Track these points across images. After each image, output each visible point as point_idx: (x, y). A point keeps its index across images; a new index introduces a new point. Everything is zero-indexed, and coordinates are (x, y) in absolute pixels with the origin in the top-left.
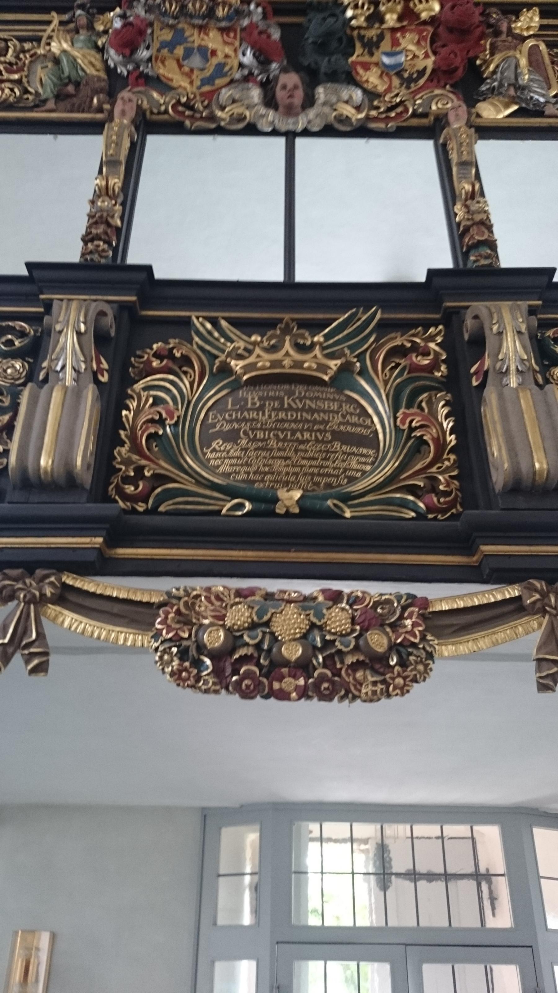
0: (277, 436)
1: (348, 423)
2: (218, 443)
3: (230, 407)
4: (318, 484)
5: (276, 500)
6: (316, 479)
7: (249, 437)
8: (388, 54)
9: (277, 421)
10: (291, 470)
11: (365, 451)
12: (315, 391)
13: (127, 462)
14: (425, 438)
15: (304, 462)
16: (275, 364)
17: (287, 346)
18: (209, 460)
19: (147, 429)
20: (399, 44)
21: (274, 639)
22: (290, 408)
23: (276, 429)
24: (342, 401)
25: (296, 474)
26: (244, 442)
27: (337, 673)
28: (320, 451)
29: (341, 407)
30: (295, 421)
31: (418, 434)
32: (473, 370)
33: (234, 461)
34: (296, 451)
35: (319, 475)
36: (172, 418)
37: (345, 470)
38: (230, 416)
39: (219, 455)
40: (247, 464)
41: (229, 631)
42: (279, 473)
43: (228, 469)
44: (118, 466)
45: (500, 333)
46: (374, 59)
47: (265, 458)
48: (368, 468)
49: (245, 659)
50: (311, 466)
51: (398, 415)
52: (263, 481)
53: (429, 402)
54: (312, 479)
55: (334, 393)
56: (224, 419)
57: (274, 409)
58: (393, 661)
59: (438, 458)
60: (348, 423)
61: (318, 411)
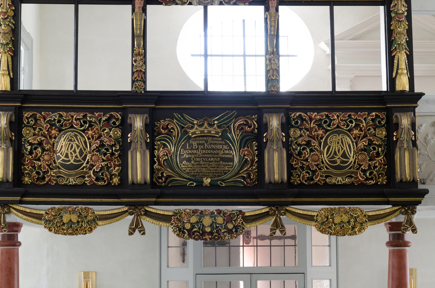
0: (203, 159)
2: (185, 162)
3: (188, 148)
4: (215, 176)
6: (215, 174)
7: (194, 160)
9: (203, 154)
10: (207, 171)
12: (215, 139)
13: (158, 170)
14: (248, 159)
15: (211, 169)
16: (202, 132)
17: (206, 124)
18: (182, 168)
19: (163, 157)
22: (207, 149)
23: (203, 157)
24: (223, 144)
25: (209, 173)
26: (193, 162)
28: (216, 165)
29: (223, 147)
30: (209, 154)
31: (246, 158)
32: (264, 135)
33: (190, 169)
34: (209, 165)
35: (216, 173)
36: (170, 155)
37: (224, 170)
38: (188, 152)
39: (185, 166)
40: (194, 170)
42: (204, 172)
43: (189, 171)
44: (155, 171)
45: (272, 129)
47: (199, 167)
48: (231, 169)
50: (213, 170)
51: (240, 151)
52: (199, 175)
53: (251, 145)
54: (214, 174)
55: (221, 140)
56: (186, 153)
57: (202, 149)
59: (252, 165)
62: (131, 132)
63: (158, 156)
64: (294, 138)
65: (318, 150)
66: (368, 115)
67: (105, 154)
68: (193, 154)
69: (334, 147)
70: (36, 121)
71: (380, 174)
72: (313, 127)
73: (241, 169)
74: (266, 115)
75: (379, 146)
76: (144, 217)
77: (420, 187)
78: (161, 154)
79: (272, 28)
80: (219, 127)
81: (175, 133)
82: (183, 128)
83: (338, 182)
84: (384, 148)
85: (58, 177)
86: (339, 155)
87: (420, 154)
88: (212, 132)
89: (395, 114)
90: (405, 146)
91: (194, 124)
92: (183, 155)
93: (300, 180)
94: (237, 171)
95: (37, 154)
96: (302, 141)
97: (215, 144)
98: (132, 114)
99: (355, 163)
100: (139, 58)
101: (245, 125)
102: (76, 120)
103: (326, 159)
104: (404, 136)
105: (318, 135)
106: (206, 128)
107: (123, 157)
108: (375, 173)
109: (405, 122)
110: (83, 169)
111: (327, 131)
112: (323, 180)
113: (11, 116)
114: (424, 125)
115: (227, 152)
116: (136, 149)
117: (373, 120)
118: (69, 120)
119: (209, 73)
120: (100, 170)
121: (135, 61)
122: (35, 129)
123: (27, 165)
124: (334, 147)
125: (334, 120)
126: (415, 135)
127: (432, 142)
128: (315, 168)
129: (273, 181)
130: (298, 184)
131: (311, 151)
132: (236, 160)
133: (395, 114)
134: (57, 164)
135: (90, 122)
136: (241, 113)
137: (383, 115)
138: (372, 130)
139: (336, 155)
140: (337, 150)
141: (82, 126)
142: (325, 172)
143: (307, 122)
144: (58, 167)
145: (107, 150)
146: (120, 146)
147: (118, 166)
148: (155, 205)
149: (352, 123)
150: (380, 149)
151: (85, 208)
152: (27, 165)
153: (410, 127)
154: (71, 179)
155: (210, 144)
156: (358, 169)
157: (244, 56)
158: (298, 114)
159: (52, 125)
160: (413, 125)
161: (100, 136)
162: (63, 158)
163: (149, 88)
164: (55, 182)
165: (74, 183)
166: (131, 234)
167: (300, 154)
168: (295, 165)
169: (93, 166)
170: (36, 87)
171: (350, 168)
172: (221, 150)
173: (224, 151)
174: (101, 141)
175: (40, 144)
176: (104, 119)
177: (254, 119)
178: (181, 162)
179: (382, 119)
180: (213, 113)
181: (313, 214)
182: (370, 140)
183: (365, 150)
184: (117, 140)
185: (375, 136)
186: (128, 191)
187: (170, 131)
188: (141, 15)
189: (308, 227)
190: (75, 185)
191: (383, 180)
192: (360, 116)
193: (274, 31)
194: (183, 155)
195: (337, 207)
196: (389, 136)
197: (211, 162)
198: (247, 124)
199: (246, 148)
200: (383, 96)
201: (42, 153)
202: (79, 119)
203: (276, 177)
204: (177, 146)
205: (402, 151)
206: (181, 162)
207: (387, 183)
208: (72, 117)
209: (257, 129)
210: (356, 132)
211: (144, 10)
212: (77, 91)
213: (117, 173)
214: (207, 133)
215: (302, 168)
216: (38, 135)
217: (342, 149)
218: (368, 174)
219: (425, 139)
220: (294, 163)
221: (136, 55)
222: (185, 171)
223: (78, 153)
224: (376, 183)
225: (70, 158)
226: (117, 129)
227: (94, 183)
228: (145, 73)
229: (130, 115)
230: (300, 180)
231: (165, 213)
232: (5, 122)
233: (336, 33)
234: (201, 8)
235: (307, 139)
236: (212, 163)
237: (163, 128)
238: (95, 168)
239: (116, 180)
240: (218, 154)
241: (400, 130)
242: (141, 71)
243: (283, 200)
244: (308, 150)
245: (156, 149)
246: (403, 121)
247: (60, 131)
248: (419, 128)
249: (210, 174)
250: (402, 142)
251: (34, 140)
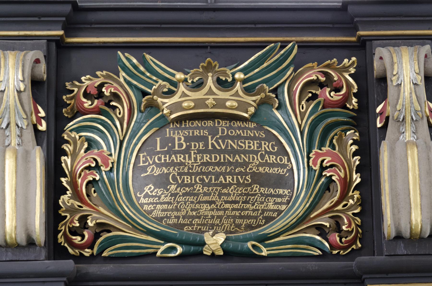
0: (202, 180)
2: (150, 188)
3: (158, 149)
4: (239, 226)
5: (203, 244)
6: (238, 221)
7: (178, 181)
9: (203, 164)
10: (215, 213)
11: (281, 191)
13: (72, 210)
14: (334, 178)
15: (227, 206)
16: (199, 103)
17: (210, 83)
18: (142, 205)
19: (86, 175)
23: (202, 173)
24: (261, 139)
25: (219, 217)
26: (173, 187)
28: (241, 195)
29: (260, 146)
30: (219, 164)
31: (328, 175)
33: (165, 206)
34: (220, 195)
35: (241, 217)
36: (107, 166)
37: (263, 211)
38: (160, 159)
39: (151, 200)
40: (177, 210)
42: (205, 217)
43: (161, 214)
44: (63, 214)
47: (192, 202)
48: (284, 207)
50: (233, 209)
51: (311, 155)
52: (191, 224)
53: (340, 140)
54: (234, 222)
55: (255, 128)
56: (154, 163)
57: (199, 151)
61: (239, 152)
68: (173, 164)
80: (248, 91)
82: (145, 94)
88: (228, 104)
91: (175, 84)
94: (300, 211)
97: (239, 137)
101: (322, 85)
115: (273, 159)
155: (223, 138)
172: (255, 153)
173: (262, 157)
194: (144, 169)
197: (225, 186)
199: (326, 149)
209: (355, 95)
214: (214, 107)
222: (150, 212)
236: (230, 190)
240: (245, 164)
245: (65, 154)
249: (224, 221)
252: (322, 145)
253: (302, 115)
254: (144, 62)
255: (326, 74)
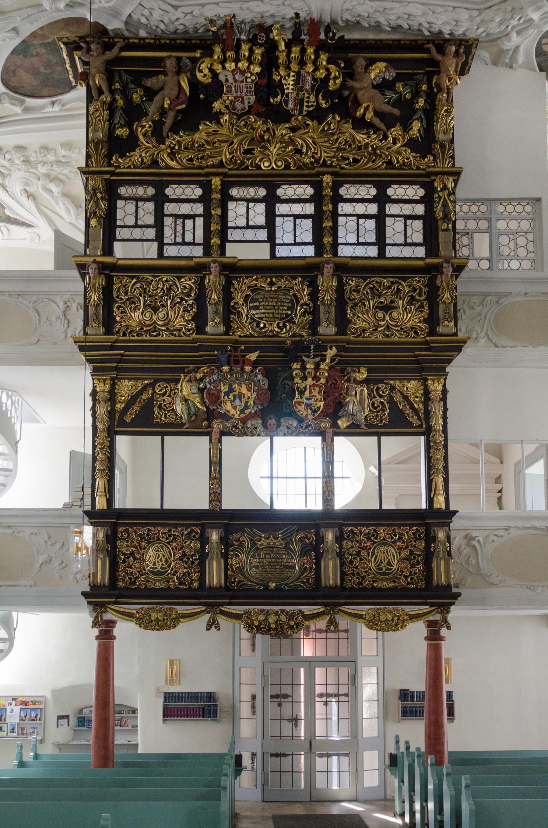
1: (288, 562)
8: (307, 399)
13: (231, 576)
16: (268, 544)
17: (272, 538)
20: (312, 393)
21: (269, 623)
22: (273, 558)
27: (283, 630)
30: (274, 562)
41: (259, 621)
46: (302, 400)
49: (263, 628)
57: (268, 558)
58: (295, 627)
59: (310, 572)
60: (288, 562)
61: (280, 559)
62: (208, 543)
63: (231, 564)
64: (347, 549)
65: (366, 559)
66: (410, 529)
67: (187, 563)
68: (260, 562)
69: (381, 556)
70: (128, 535)
71: (420, 579)
72: (363, 540)
73: (301, 575)
74: (322, 530)
75: (419, 555)
76: (219, 615)
77: (454, 590)
78: (234, 563)
79: (329, 456)
80: (283, 539)
81: (246, 545)
82: (252, 540)
83: (383, 586)
84: (424, 557)
85: (147, 582)
86: (385, 563)
87: (454, 562)
89: (433, 528)
90: (441, 556)
91: (262, 537)
92: (252, 563)
93: (351, 584)
95: (129, 563)
96: (353, 551)
97: (280, 554)
98: (209, 528)
99: (398, 570)
100: (215, 481)
102: (162, 533)
103: (373, 567)
104: (441, 547)
105: (367, 546)
106: (272, 540)
107: (202, 564)
108: (415, 578)
109: (441, 535)
110: (168, 575)
111: (375, 543)
112: (371, 584)
113: (107, 531)
114: (458, 538)
115: (289, 560)
116: (212, 559)
117: (413, 533)
118: (156, 534)
119: (274, 493)
120: (183, 576)
121: (212, 484)
122: (127, 541)
123: (121, 571)
124: (381, 556)
125: (381, 533)
126: (450, 547)
127: (465, 552)
128: (364, 574)
129: (328, 585)
130: (350, 588)
131: (361, 559)
132: (297, 567)
133: (433, 528)
134: (147, 571)
135: (174, 535)
136: (302, 528)
137: (422, 529)
138: (413, 542)
139: (382, 563)
140: (383, 559)
141: (167, 539)
142: (372, 578)
143: (357, 535)
144: (147, 573)
145: (189, 559)
146: (199, 556)
147: (198, 572)
148: (228, 605)
149: (396, 536)
150: (420, 558)
151: (170, 608)
152: (121, 571)
153: (445, 540)
154: (158, 584)
155: (275, 554)
156: (400, 575)
157: (306, 478)
158: (350, 528)
159: (142, 538)
160: (448, 538)
161: (182, 547)
162: (151, 565)
163: (224, 507)
164: (144, 586)
165: (160, 586)
166: (208, 629)
167: (351, 562)
168: (347, 571)
169: (176, 572)
170: (129, 505)
171: (394, 575)
174: (184, 552)
175: (132, 554)
176: (186, 533)
177: (312, 533)
178: (251, 569)
179: (422, 533)
180: (277, 528)
181: (362, 613)
182: (411, 550)
183: (407, 559)
184: (196, 550)
185: (415, 547)
186: (206, 593)
187: (241, 543)
188: (217, 445)
189: (359, 624)
190: (162, 589)
191: (422, 585)
192: (403, 530)
193: (330, 458)
194: (252, 563)
195: (382, 607)
196: (428, 547)
197: (276, 569)
198: (307, 537)
200: (422, 513)
201: (134, 561)
202: (165, 533)
203: (331, 582)
204: (247, 554)
205: (439, 561)
206: (251, 569)
207: (425, 587)
208: (159, 531)
210: (399, 543)
211: (220, 441)
212: (163, 509)
213: (197, 579)
215: (353, 574)
216: (130, 546)
217: (387, 558)
218: (409, 579)
219: (459, 549)
220: (346, 570)
221: (213, 479)
223: (163, 562)
224: (416, 587)
225: (157, 566)
226: (197, 541)
227: (178, 587)
228: (220, 494)
229: (207, 530)
230: (351, 584)
231: (238, 612)
232: (102, 536)
233: (382, 459)
234: (268, 440)
235: (357, 550)
237: (235, 541)
238: (178, 574)
239: (196, 585)
240: (281, 562)
241: (437, 542)
242: (217, 492)
243: (337, 601)
244: (358, 559)
245: (229, 558)
246: (439, 535)
247: (149, 543)
248: (453, 540)
250: (438, 552)
251: (127, 550)
252: (304, 556)
253: (299, 546)
254: (252, 531)
255: (305, 534)
